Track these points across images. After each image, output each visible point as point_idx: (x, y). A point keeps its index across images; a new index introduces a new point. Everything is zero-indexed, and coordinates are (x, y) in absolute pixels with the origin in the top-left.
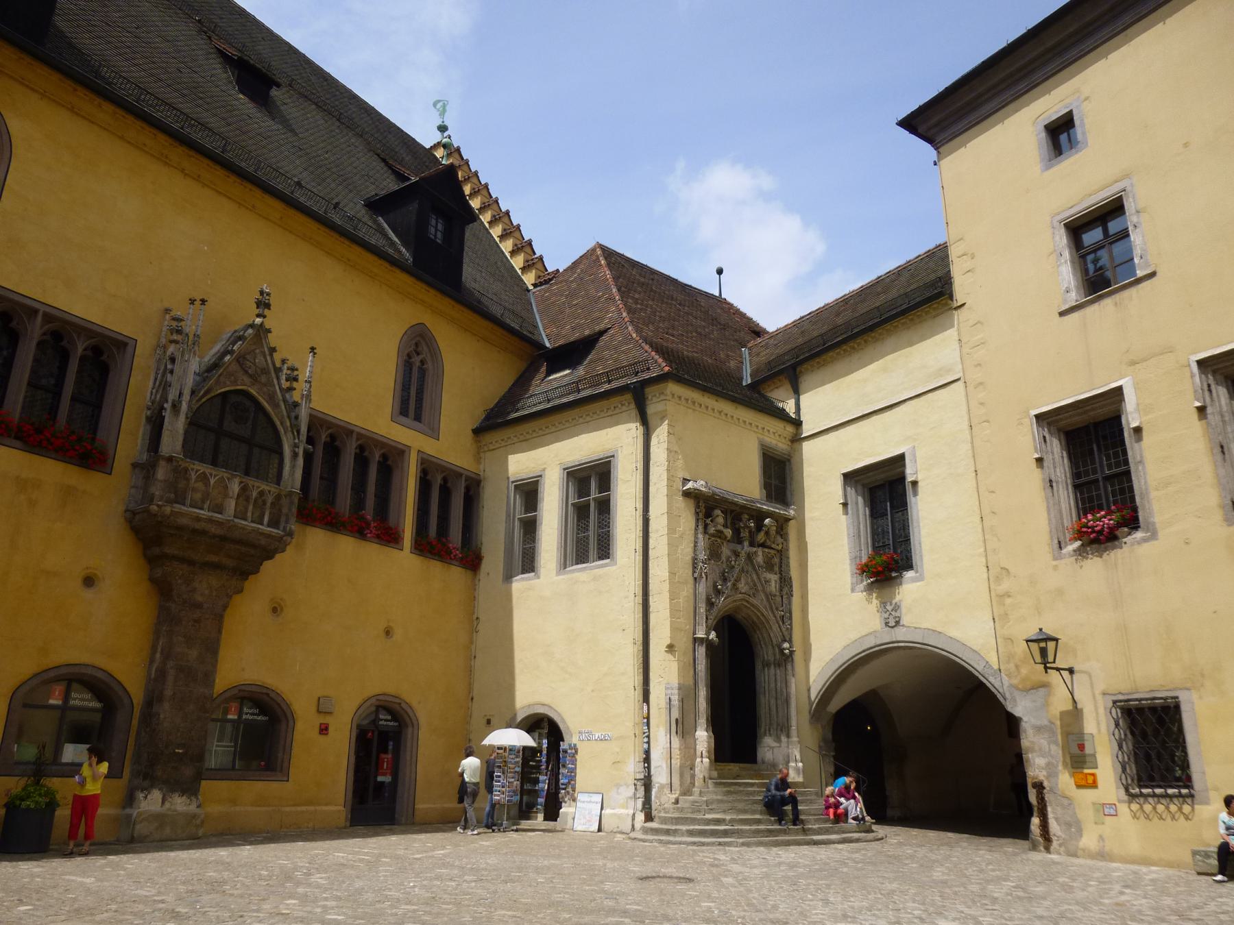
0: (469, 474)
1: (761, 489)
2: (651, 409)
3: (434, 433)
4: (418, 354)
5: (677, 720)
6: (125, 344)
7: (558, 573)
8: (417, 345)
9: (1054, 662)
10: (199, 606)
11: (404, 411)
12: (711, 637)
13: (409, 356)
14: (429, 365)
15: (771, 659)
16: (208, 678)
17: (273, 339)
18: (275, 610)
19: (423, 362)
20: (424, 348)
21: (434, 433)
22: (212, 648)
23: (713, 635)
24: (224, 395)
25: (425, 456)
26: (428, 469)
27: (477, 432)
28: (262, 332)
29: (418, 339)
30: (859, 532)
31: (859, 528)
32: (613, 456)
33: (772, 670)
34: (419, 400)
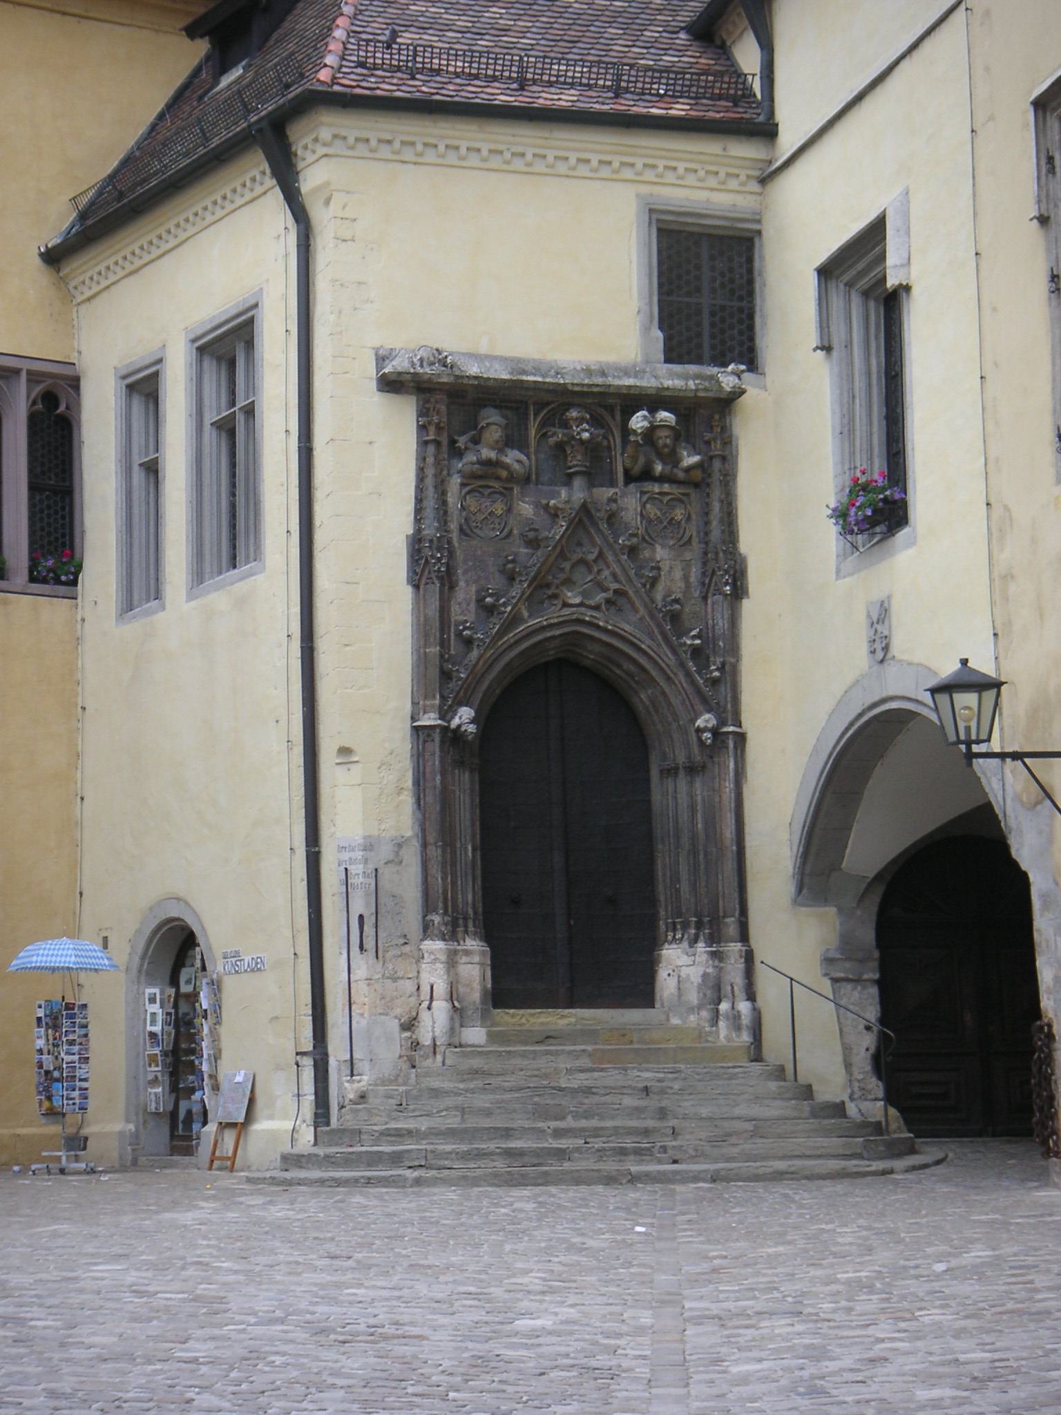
0: (37, 366)
1: (646, 330)
2: (311, 179)
5: (361, 917)
7: (190, 598)
9: (989, 740)
12: (455, 722)
15: (681, 759)
23: (464, 717)
27: (54, 258)
30: (852, 420)
31: (851, 411)
32: (256, 306)
33: (682, 783)
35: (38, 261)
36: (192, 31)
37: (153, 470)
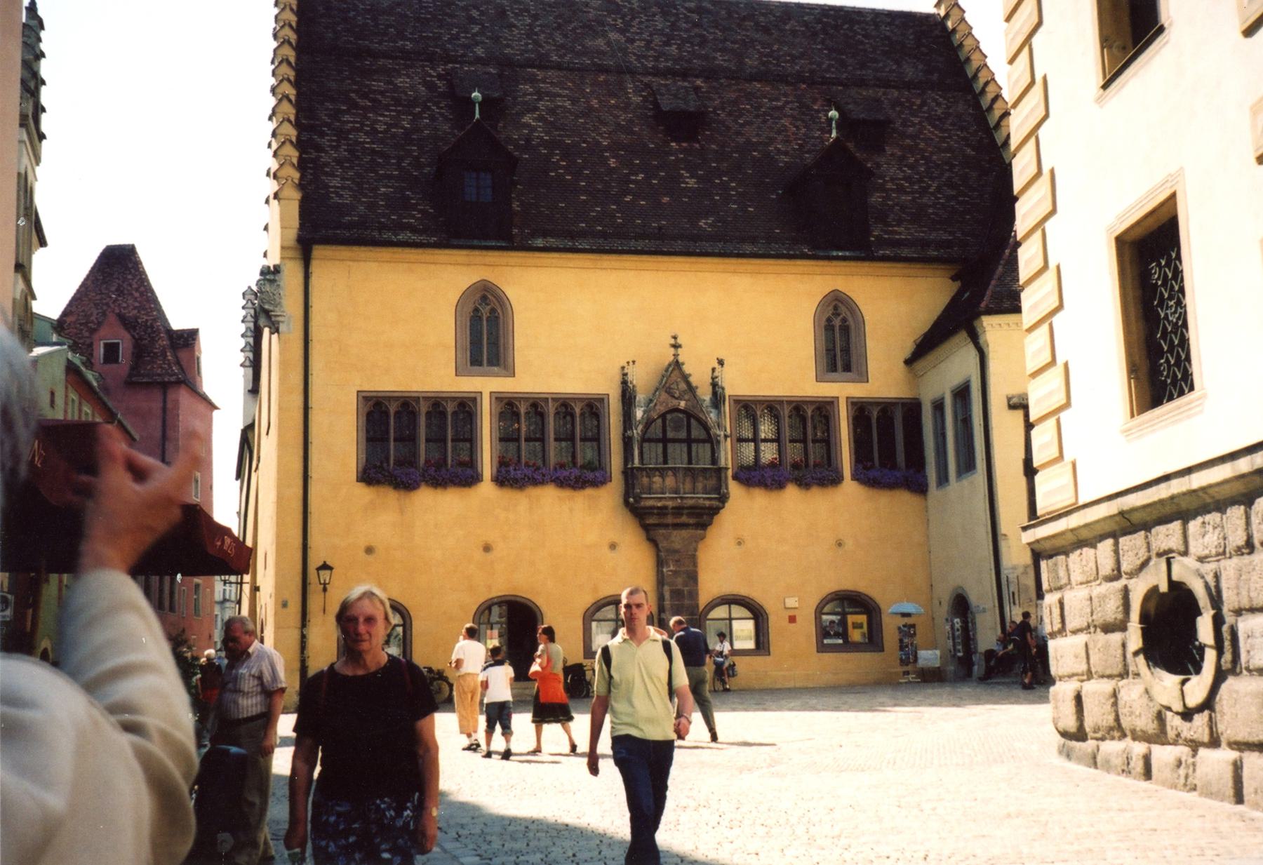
3: (863, 377)
4: (839, 315)
6: (603, 399)
8: (836, 308)
10: (676, 551)
11: (832, 367)
13: (829, 320)
14: (851, 322)
16: (694, 595)
17: (687, 369)
18: (739, 543)
19: (844, 320)
20: (843, 309)
21: (863, 377)
22: (693, 577)
24: (663, 416)
25: (855, 400)
26: (860, 410)
27: (909, 362)
28: (677, 364)
29: (834, 304)
34: (846, 350)
35: (902, 364)
36: (954, 278)
37: (944, 435)
